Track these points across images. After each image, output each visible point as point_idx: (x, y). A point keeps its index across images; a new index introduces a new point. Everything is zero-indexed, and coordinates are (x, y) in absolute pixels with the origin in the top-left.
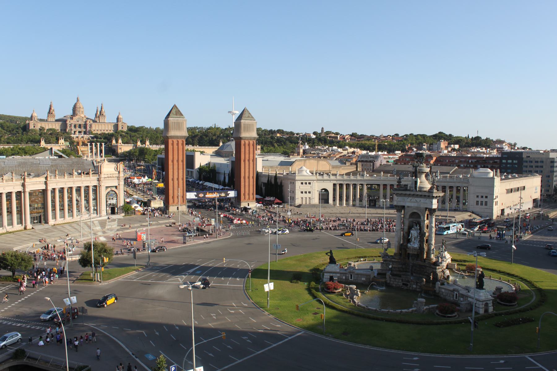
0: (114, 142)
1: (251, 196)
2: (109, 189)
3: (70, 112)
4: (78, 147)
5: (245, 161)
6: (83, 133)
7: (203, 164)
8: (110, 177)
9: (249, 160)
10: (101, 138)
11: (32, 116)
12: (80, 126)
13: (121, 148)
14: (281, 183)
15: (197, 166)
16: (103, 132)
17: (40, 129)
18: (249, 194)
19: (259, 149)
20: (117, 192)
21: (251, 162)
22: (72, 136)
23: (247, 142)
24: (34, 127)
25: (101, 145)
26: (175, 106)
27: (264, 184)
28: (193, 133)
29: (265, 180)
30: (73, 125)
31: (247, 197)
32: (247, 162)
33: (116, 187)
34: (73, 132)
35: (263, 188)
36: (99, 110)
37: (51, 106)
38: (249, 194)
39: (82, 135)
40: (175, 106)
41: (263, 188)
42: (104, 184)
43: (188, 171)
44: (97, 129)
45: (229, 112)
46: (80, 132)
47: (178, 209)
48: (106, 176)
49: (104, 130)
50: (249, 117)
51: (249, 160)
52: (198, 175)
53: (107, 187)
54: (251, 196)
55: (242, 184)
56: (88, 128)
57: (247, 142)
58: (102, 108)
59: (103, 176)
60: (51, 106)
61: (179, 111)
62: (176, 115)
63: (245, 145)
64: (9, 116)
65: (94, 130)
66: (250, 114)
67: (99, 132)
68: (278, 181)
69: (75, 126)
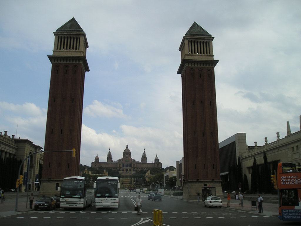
24: (96, 166)
27: (249, 168)
56: (133, 166)
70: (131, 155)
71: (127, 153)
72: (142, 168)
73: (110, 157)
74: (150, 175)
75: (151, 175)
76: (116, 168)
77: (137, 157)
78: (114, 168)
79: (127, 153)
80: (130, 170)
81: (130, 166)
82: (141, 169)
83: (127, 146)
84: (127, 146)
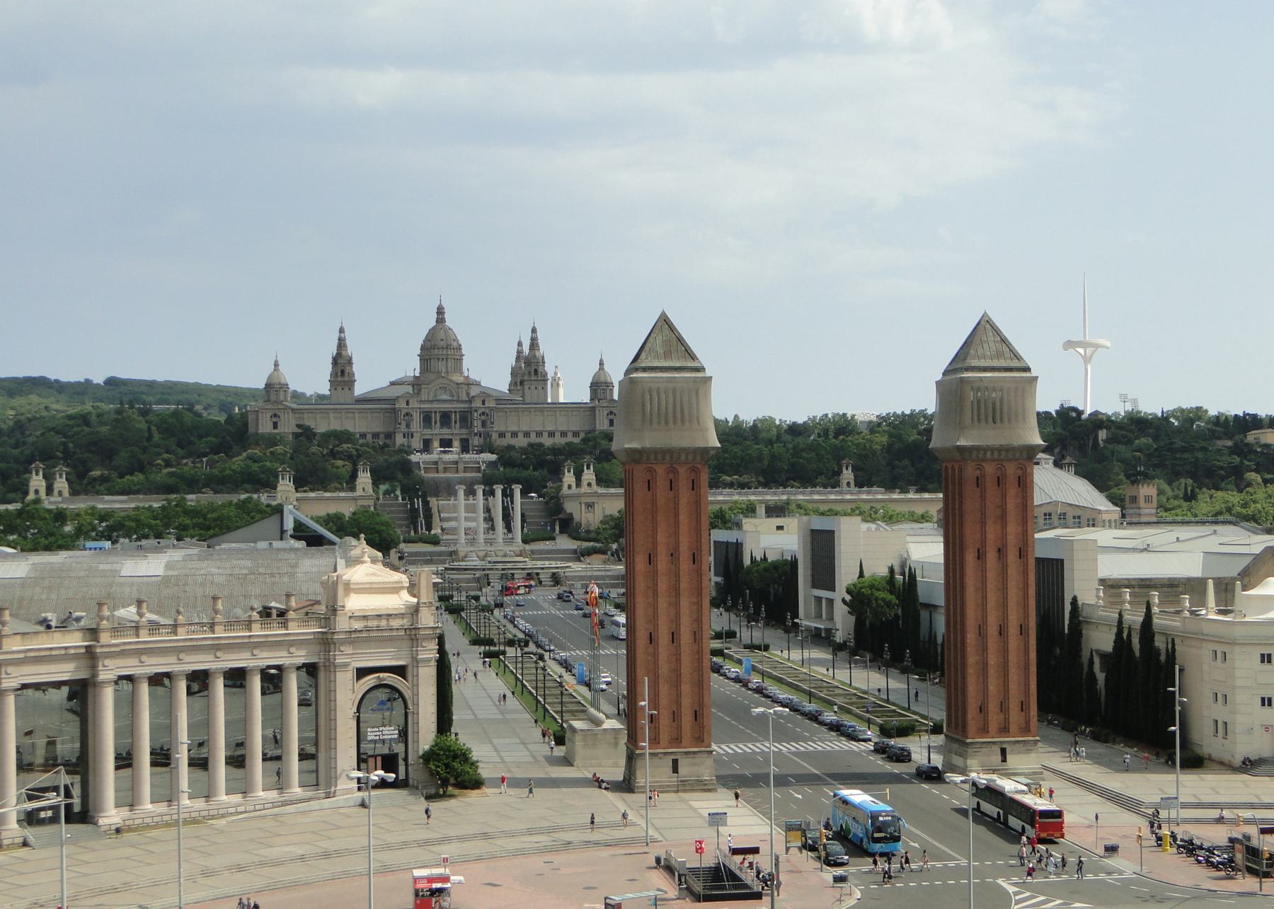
0: (569, 478)
1: (1015, 716)
2: (370, 680)
3: (410, 366)
4: (433, 502)
5: (980, 555)
6: (456, 447)
7: (878, 568)
8: (374, 630)
9: (1001, 552)
10: (523, 466)
11: (269, 386)
12: (446, 418)
13: (590, 506)
14: (1172, 656)
15: (846, 575)
16: (533, 439)
17: (296, 435)
18: (1003, 707)
19: (1148, 499)
20: (407, 694)
21: (1012, 556)
22: (415, 458)
23: (990, 469)
24: (275, 425)
25: (508, 494)
26: (664, 322)
27: (1104, 656)
28: (899, 438)
29: (1101, 640)
30: (417, 417)
31: (994, 719)
32: (991, 556)
33: (400, 671)
34: (417, 443)
35: (1101, 677)
36: (526, 349)
37: (341, 344)
38: (1003, 707)
39: (454, 454)
40: (664, 322)
41: (1101, 677)
42: (350, 658)
43: (819, 599)
44: (519, 430)
45: (1069, 345)
46: (446, 443)
47: (675, 770)
48: (358, 625)
49: (539, 434)
50: (999, 355)
51: (1001, 552)
52: (853, 619)
53: (362, 673)
54: (1015, 716)
55: (972, 659)
56: (477, 426)
57: (990, 469)
58: (534, 344)
59: (342, 624)
60: (341, 344)
61: (680, 340)
62: (667, 355)
63: (979, 482)
64: (219, 390)
65: (502, 435)
66: (1004, 341)
67: (521, 442)
68: (1160, 643)
69: (427, 419)
70: (466, 363)
71: (439, 349)
72: (527, 434)
73: (342, 368)
74: (595, 487)
75: (601, 490)
76: (390, 436)
77: (489, 369)
78: (376, 435)
79: (439, 349)
80: (465, 448)
81: (465, 418)
82: (521, 435)
83: (440, 311)
84: (440, 311)
